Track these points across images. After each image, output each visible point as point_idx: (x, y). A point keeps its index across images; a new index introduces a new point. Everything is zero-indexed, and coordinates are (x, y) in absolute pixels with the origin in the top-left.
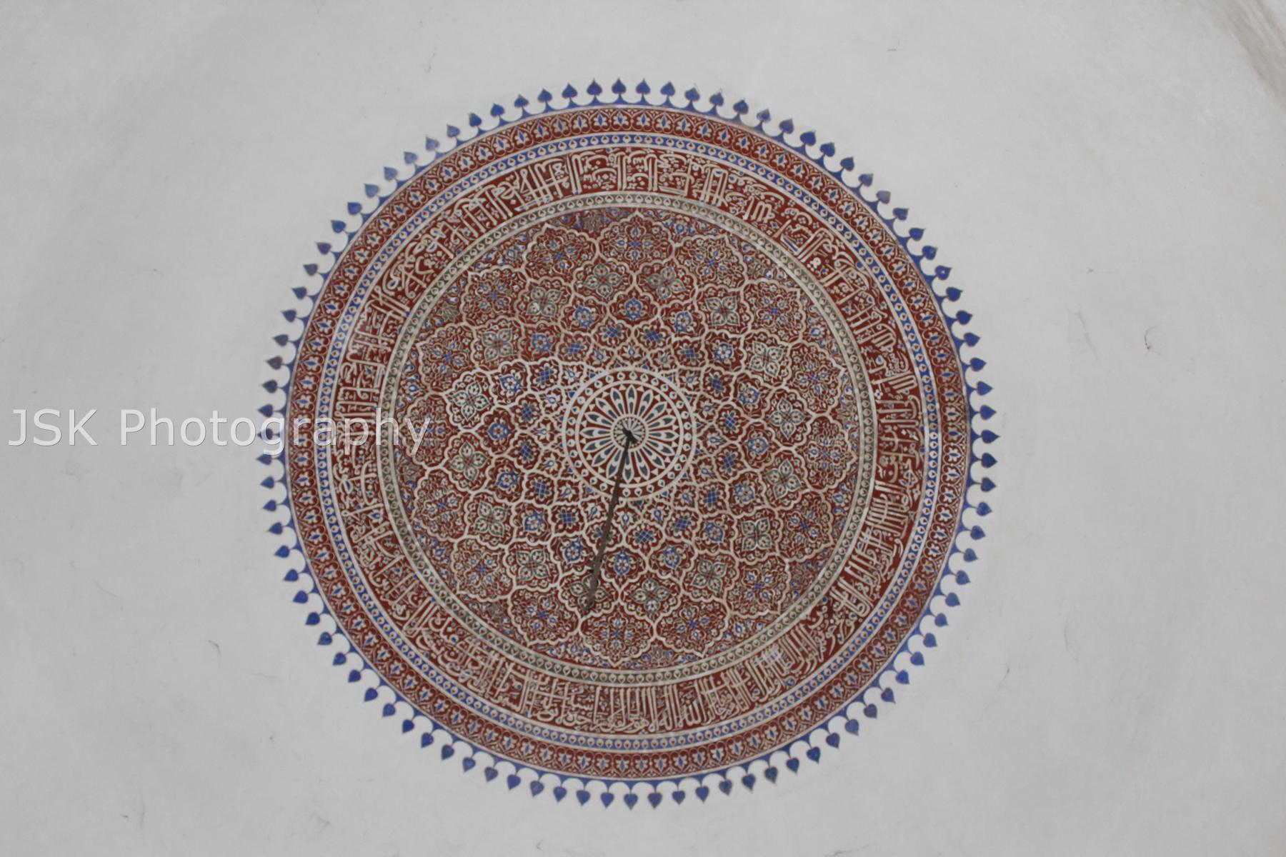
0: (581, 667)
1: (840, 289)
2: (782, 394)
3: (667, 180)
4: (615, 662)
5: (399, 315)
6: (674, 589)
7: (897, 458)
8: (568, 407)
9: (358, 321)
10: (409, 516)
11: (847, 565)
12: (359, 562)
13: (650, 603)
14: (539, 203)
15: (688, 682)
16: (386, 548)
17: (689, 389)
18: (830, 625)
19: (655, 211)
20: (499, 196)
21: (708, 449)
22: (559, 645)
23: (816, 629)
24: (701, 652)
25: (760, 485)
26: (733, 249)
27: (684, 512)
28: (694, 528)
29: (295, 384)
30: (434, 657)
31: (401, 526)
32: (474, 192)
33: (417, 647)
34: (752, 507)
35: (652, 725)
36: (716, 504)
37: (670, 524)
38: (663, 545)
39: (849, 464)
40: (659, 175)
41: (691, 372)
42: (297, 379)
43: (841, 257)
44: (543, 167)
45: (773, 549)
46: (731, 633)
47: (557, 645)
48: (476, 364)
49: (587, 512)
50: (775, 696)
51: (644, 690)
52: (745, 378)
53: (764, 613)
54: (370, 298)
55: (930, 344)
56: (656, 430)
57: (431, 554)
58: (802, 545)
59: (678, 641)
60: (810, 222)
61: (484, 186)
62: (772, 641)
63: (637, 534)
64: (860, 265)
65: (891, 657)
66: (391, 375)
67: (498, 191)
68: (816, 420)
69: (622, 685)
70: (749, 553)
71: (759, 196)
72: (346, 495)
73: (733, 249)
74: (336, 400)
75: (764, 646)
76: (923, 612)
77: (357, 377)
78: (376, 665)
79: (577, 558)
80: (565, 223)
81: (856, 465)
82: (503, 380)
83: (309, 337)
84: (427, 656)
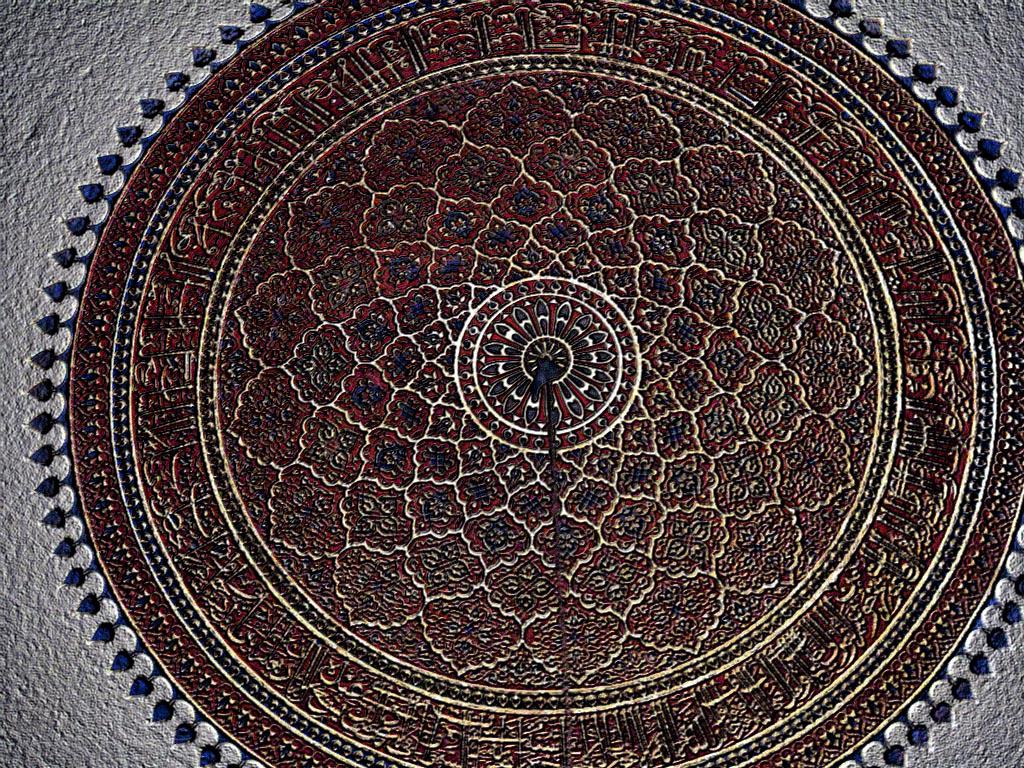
0: (535, 693)
1: (820, 149)
2: (752, 287)
3: (548, 35)
4: (579, 677)
5: (203, 280)
6: (639, 565)
7: (932, 370)
8: (458, 344)
9: (145, 304)
10: (266, 539)
11: (878, 513)
12: (209, 617)
13: (613, 588)
14: (370, 95)
15: (685, 690)
16: (246, 590)
17: (620, 293)
18: (867, 595)
19: (539, 77)
20: (313, 99)
21: (659, 370)
22: (502, 664)
23: (847, 602)
24: (693, 647)
25: (740, 411)
26: (658, 110)
27: (639, 457)
28: (655, 478)
29: (75, 409)
30: (334, 719)
31: (258, 553)
32: (275, 100)
33: (310, 712)
34: (733, 442)
35: (643, 759)
36: (680, 441)
37: (623, 476)
38: (618, 507)
39: (862, 377)
40: (536, 33)
41: (619, 271)
42: (78, 403)
43: (814, 109)
44: (367, 49)
45: (771, 497)
46: (730, 617)
47: (496, 668)
48: (321, 317)
49: (505, 478)
50: (805, 701)
51: (623, 712)
52: (695, 273)
53: (773, 585)
54: (156, 269)
55: (962, 214)
56: (582, 353)
57: (306, 581)
58: (812, 487)
59: (659, 636)
60: (765, 65)
61: (287, 91)
62: (788, 623)
63: (579, 496)
64: (849, 119)
65: (962, 635)
66: (207, 360)
67: (308, 92)
68: (807, 321)
69: (594, 709)
70: (737, 504)
71: (686, 39)
72: (175, 533)
73: (658, 110)
74: (136, 414)
75: (779, 631)
76: (996, 573)
77: (159, 376)
78: (258, 752)
79: (503, 543)
80: (413, 114)
81: (873, 375)
82: (363, 330)
83: (83, 345)
84: (325, 721)
